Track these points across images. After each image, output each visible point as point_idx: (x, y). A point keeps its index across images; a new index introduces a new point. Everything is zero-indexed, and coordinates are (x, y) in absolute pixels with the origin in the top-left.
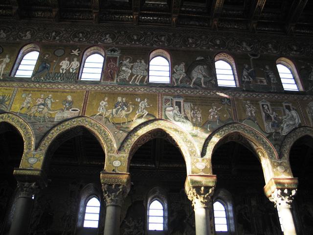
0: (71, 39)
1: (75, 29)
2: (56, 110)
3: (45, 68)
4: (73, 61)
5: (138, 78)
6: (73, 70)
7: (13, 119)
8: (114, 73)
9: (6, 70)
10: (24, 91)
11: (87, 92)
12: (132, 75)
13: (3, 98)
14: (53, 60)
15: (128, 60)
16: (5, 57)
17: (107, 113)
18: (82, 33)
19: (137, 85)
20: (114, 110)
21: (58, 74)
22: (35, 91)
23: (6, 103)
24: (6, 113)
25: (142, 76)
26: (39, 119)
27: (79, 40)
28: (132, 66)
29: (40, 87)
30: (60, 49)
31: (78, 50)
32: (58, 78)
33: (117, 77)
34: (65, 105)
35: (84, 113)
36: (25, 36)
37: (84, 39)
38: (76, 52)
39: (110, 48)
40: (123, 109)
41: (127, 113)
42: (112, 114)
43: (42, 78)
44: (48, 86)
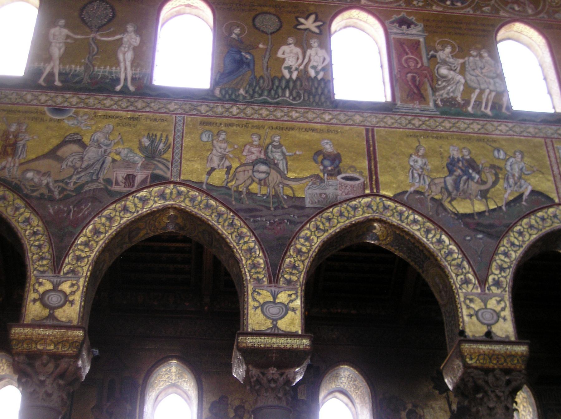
4: (310, 47)
5: (484, 97)
6: (317, 73)
7: (193, 199)
8: (422, 83)
10: (202, 123)
11: (367, 131)
12: (468, 89)
13: (152, 142)
14: (259, 43)
15: (448, 50)
16: (125, 31)
17: (433, 188)
19: (488, 116)
20: (450, 181)
21: (280, 81)
22: (231, 125)
23: (165, 156)
24: (171, 183)
25: (493, 94)
26: (264, 201)
28: (463, 65)
29: (242, 115)
32: (284, 91)
33: (434, 94)
34: (322, 163)
35: (378, 189)
38: (309, 24)
39: (395, 17)
40: (470, 178)
41: (483, 187)
42: (447, 189)
43: (242, 91)
44: (264, 112)
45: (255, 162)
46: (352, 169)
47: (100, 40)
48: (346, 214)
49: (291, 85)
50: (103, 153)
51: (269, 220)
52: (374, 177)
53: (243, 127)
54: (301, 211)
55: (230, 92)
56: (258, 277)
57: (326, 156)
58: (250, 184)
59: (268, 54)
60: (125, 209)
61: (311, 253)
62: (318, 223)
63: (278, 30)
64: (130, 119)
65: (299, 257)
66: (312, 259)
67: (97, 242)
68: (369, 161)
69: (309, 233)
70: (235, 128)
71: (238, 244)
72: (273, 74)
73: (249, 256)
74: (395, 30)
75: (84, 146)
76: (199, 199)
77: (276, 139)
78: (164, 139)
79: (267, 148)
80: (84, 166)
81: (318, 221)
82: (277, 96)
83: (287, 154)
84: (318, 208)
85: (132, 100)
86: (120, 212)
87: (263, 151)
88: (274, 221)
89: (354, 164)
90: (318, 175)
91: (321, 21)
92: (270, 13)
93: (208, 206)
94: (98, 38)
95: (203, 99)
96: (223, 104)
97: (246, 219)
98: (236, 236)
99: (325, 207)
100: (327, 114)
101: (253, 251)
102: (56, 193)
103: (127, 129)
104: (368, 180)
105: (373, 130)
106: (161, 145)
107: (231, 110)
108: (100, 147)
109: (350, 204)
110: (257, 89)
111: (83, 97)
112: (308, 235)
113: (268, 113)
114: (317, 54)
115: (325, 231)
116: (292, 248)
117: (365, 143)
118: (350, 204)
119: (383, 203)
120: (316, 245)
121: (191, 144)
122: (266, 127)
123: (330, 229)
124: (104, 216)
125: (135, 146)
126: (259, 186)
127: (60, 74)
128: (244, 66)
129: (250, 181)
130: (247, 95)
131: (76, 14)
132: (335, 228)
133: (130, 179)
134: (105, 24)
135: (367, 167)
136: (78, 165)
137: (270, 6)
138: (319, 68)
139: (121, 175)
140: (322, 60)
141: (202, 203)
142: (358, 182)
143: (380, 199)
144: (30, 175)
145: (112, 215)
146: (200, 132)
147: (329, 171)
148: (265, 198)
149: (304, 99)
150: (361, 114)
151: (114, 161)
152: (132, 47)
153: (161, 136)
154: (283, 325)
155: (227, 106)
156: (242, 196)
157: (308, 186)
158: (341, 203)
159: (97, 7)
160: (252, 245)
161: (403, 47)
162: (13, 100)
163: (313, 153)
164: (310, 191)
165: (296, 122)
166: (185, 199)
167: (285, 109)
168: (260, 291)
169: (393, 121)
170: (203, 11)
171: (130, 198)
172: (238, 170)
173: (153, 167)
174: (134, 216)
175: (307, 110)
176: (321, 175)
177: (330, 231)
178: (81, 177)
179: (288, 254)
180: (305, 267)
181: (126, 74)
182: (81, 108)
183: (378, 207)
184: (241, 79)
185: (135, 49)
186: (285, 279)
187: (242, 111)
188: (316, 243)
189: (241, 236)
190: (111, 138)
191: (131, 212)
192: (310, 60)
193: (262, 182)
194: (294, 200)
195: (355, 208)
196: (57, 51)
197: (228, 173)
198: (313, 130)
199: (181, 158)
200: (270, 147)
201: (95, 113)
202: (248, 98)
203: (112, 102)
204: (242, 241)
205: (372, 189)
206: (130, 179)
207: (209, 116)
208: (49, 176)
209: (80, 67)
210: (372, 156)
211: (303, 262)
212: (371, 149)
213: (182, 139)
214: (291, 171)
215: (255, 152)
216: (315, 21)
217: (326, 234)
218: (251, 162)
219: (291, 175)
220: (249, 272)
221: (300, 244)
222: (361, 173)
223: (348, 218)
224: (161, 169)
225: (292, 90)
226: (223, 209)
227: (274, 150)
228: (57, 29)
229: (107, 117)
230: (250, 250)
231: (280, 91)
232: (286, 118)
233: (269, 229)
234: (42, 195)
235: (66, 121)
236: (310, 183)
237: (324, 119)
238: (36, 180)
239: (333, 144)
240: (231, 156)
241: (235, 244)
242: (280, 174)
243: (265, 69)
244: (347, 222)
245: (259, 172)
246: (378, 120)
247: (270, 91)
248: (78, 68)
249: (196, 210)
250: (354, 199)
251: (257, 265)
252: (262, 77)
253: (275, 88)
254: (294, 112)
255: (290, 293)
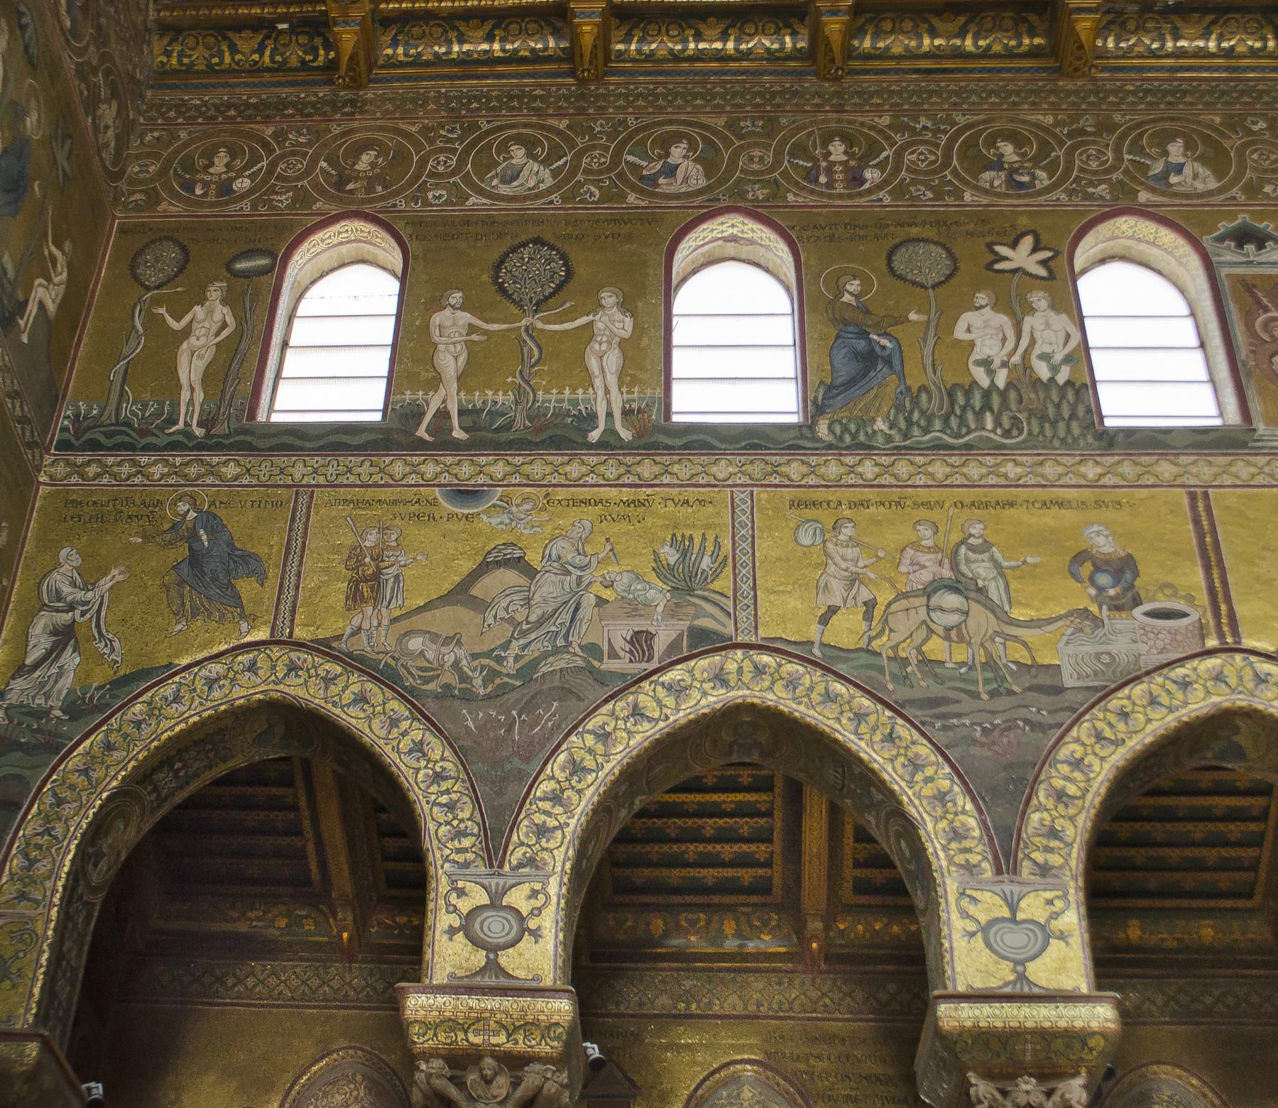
0: (467, 178)
1: (961, 120)
2: (1050, 621)
3: (869, 359)
4: (1031, 310)
6: (1055, 369)
7: (792, 684)
9: (635, 381)
11: (1193, 497)
13: (685, 554)
14: (909, 311)
18: (1018, 140)
21: (968, 393)
22: (864, 504)
23: (716, 585)
26: (962, 678)
27: (1012, 183)
30: (917, 240)
31: (1028, 242)
32: (979, 415)
34: (1092, 580)
36: (671, 171)
37: (1041, 174)
38: (1022, 257)
39: (1224, 226)
43: (880, 425)
44: (939, 469)
45: (929, 590)
46: (1168, 591)
47: (542, 330)
48: (1164, 699)
49: (996, 401)
50: (574, 585)
51: (980, 724)
52: (1223, 608)
53: (894, 508)
54: (1055, 698)
55: (853, 427)
56: (967, 861)
57: (1100, 565)
58: (926, 640)
59: (932, 333)
60: (637, 712)
61: (1089, 796)
62: (1100, 725)
63: (949, 277)
64: (627, 504)
65: (1061, 808)
66: (1093, 811)
67: (579, 792)
68: (1207, 568)
69: (1078, 750)
70: (873, 509)
71: (911, 783)
72: (950, 380)
73: (939, 811)
74: (1229, 257)
75: (530, 572)
76: (807, 681)
77: (973, 531)
78: (710, 547)
79: (956, 552)
80: (533, 618)
81: (1099, 718)
82: (964, 430)
83: (1005, 564)
84: (1095, 689)
85: (629, 460)
86: (626, 720)
87: (946, 561)
88: (991, 724)
89: (1170, 579)
90: (1086, 610)
91: (1050, 249)
92: (925, 240)
93: (829, 697)
94: (540, 325)
95: (790, 447)
96: (841, 455)
97: (923, 723)
98: (904, 766)
99: (1113, 686)
100: (1090, 463)
101: (947, 798)
102: (478, 682)
103: (624, 526)
104: (1209, 616)
105: (1206, 495)
106: (706, 562)
107: (860, 469)
108: (568, 573)
109: (1172, 675)
110: (916, 416)
111: (518, 460)
112: (1078, 755)
113: (948, 470)
114: (1048, 325)
115: (1118, 743)
116: (1042, 786)
117: (1191, 527)
118: (1172, 675)
119: (1253, 668)
120: (1100, 779)
121: (774, 554)
122: (947, 505)
123: (1130, 738)
124: (589, 732)
125: (646, 566)
126: (946, 643)
127: (462, 412)
128: (880, 367)
129: (923, 632)
130: (893, 432)
131: (485, 277)
132: (1141, 736)
133: (641, 641)
134: (552, 295)
135: (1203, 584)
136: (519, 618)
137: (924, 223)
138: (1059, 357)
139: (620, 633)
140: (1062, 340)
141: (816, 691)
142: (1185, 621)
143: (1245, 659)
144: (415, 644)
145: (609, 729)
146: (792, 525)
147: (1112, 598)
148: (963, 670)
149: (1030, 433)
150: (1172, 458)
151: (601, 602)
152: (617, 339)
153: (704, 539)
154: (1042, 973)
155: (850, 460)
156: (909, 669)
157: (1065, 638)
158: (1148, 673)
159: (530, 258)
160: (946, 784)
161: (1253, 295)
162: (365, 478)
163: (1068, 558)
164: (1070, 649)
165: (1017, 486)
166: (773, 683)
167: (989, 458)
168: (975, 894)
169: (1253, 470)
170: (768, 248)
171: (645, 685)
172: (893, 608)
173: (691, 610)
174: (658, 727)
175: (1041, 458)
176: (1094, 609)
177: (1130, 743)
178: (530, 643)
179: (1034, 801)
180: (1079, 831)
181: (609, 402)
182: (514, 485)
183: (1241, 678)
184: (876, 396)
185: (623, 344)
186: (1035, 862)
187: (886, 469)
188: (1099, 774)
189: (915, 765)
190: (589, 550)
191: (650, 720)
192: (1033, 342)
193: (953, 634)
194: (1033, 671)
195: (1185, 685)
196: (450, 362)
197: (868, 616)
198: (1061, 504)
199: (754, 588)
200: (963, 550)
201: (547, 495)
202: (897, 438)
203: (584, 469)
204: (919, 777)
205: (1221, 636)
206: (641, 641)
207: (811, 486)
208: (459, 643)
209: (505, 393)
210: (1211, 557)
211: (1072, 819)
212: (1208, 539)
213: (753, 543)
214: (1020, 603)
215: (928, 564)
216: (1035, 250)
217: (1122, 750)
218: (921, 587)
219: (1017, 613)
220: (945, 848)
221: (1059, 776)
222: (1190, 599)
223: (1171, 709)
224: (712, 616)
225: (1000, 413)
226: (866, 702)
227: (970, 554)
228: (448, 312)
229: (575, 502)
230: (941, 797)
231: (970, 417)
232: (992, 480)
233: (983, 745)
234: (447, 686)
235: (485, 518)
236: (1070, 631)
237: (1084, 477)
238: (430, 655)
239: (1114, 534)
240: (872, 576)
241: (903, 784)
242: (993, 612)
243: (929, 369)
244: (1170, 718)
245: (942, 610)
246: (1216, 470)
247: (946, 420)
248: (500, 398)
249: (802, 708)
250: (1180, 661)
251: (960, 831)
252: (923, 388)
253: (958, 411)
254: (1010, 465)
255: (1049, 895)
